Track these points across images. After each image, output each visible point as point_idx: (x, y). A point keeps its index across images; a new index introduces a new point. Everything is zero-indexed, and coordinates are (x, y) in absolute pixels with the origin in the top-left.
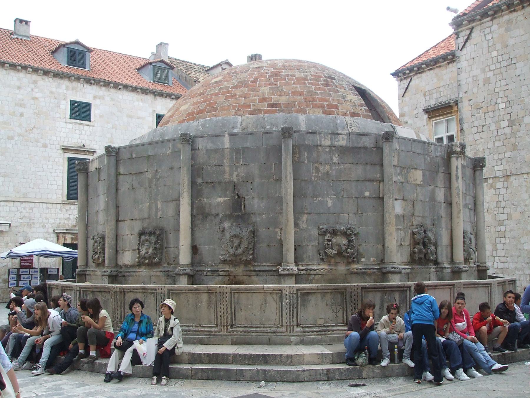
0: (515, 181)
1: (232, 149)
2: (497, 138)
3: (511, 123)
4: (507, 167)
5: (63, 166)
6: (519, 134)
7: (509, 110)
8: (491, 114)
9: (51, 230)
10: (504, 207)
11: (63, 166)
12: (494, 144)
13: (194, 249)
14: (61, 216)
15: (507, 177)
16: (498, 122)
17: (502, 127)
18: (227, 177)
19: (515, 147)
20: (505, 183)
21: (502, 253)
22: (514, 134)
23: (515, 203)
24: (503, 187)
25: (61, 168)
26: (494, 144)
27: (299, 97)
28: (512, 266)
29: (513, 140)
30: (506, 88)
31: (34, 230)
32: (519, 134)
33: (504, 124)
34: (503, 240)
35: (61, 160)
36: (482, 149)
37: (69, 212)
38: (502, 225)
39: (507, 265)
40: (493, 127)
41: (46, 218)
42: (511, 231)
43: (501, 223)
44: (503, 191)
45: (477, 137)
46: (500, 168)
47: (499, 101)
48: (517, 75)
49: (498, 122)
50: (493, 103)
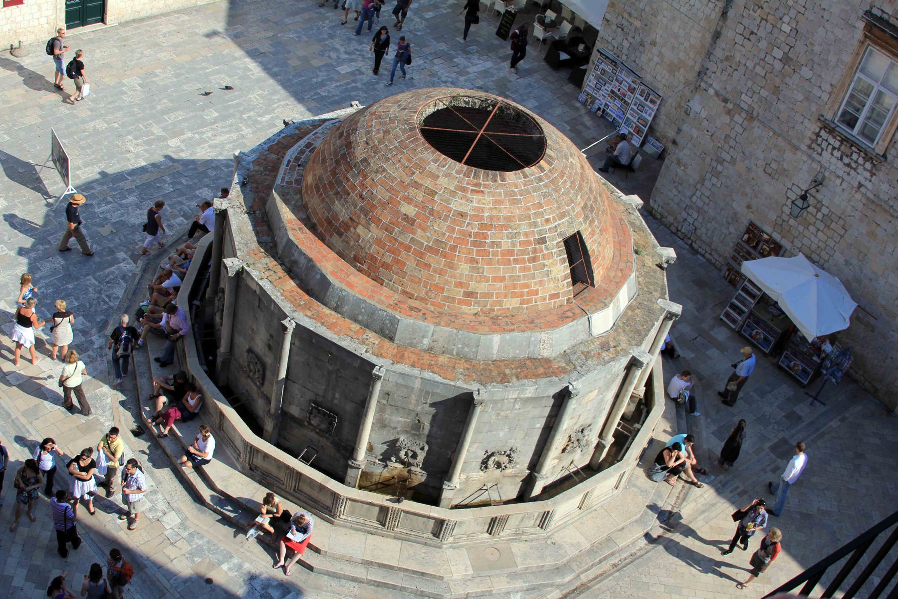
0: (757, 130)
1: (421, 390)
2: (762, 63)
3: (786, 60)
4: (756, 107)
6: (787, 80)
7: (791, 41)
8: (769, 27)
10: (731, 147)
12: (755, 67)
15: (751, 117)
16: (773, 45)
17: (773, 54)
18: (411, 407)
19: (776, 90)
20: (746, 122)
21: (707, 193)
23: (747, 153)
24: (741, 125)
26: (755, 67)
27: (498, 284)
28: (711, 213)
29: (777, 81)
30: (802, 10)
32: (787, 80)
33: (778, 53)
34: (714, 180)
36: (738, 60)
38: (721, 164)
39: (706, 208)
40: (763, 45)
43: (720, 161)
44: (740, 130)
45: (739, 39)
46: (749, 101)
47: (786, 19)
48: (823, 6)
49: (773, 45)
50: (778, 15)
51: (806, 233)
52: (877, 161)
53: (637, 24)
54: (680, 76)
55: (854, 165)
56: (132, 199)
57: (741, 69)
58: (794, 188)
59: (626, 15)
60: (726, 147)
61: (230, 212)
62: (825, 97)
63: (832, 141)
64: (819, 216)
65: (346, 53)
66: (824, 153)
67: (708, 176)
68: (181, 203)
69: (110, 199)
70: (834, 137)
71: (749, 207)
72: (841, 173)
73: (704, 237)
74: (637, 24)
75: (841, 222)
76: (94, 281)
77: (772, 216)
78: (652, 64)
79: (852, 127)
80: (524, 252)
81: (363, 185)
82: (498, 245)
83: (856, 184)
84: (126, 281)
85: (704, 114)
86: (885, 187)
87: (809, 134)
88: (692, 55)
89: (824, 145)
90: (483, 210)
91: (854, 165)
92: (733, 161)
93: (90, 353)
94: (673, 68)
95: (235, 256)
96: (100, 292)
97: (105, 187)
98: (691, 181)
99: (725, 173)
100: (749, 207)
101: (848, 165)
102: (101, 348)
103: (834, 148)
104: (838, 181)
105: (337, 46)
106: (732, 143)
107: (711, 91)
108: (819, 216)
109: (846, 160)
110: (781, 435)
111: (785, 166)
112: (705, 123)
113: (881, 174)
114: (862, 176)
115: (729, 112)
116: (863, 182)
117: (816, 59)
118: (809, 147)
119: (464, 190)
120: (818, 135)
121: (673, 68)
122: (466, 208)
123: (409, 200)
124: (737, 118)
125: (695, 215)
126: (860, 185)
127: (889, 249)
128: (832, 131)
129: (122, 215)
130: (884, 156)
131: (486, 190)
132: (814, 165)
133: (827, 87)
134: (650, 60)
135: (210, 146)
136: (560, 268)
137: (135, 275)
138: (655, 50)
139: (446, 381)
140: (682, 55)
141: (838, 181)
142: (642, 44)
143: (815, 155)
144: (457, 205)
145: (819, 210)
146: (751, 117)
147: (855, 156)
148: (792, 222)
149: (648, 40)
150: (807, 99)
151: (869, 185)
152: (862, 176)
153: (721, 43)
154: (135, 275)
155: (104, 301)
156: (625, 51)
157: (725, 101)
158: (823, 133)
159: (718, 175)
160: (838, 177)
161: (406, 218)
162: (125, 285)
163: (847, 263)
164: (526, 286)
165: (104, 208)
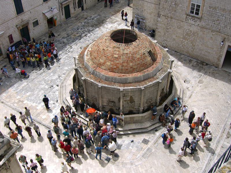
0: (174, 20)
3: (175, 4)
5: (13, 4)
6: (177, 8)
9: (15, 27)
11: (13, 4)
13: (123, 106)
14: (16, 21)
19: (175, 11)
22: (176, 8)
25: (12, 5)
29: (175, 9)
31: (10, 30)
32: (177, 8)
33: (173, 3)
34: (167, 33)
35: (12, 2)
37: (19, 19)
39: (167, 39)
41: (13, 24)
42: (170, 32)
43: (168, 29)
44: (170, 21)
45: (164, 3)
51: (190, 38)
52: (200, 19)
53: (140, 7)
54: (152, 15)
55: (196, 21)
56: (52, 74)
57: (167, 9)
58: (185, 30)
59: (137, 6)
60: (168, 26)
61: (78, 68)
62: (186, 9)
63: (190, 18)
64: (192, 33)
65: (82, 32)
66: (189, 20)
67: (166, 33)
68: (62, 72)
69: (47, 76)
70: (190, 17)
71: (176, 36)
72: (194, 23)
73: (169, 46)
74: (140, 7)
75: (197, 33)
76: (51, 93)
77: (182, 37)
78: (146, 14)
79: (193, 13)
80: (141, 57)
81: (104, 54)
82: (136, 57)
83: (197, 25)
84: (58, 91)
85: (161, 21)
86: (204, 23)
87: (185, 18)
88: (154, 10)
89: (188, 19)
90: (131, 51)
91: (196, 21)
92: (170, 28)
93: (57, 107)
94: (150, 14)
95: (83, 77)
96: (53, 95)
97: (45, 74)
98: (163, 35)
99: (169, 31)
100: (176, 36)
101: (195, 21)
102: (59, 106)
103: (191, 19)
104: (194, 25)
105: (80, 31)
106: (169, 24)
107: (162, 15)
108: (192, 33)
109: (194, 20)
110: (199, 79)
111: (182, 26)
112: (162, 22)
113: (202, 21)
114: (198, 23)
115: (166, 19)
116: (199, 24)
117: (182, 2)
118: (185, 20)
119: (126, 48)
120: (187, 17)
121: (150, 14)
122: (128, 52)
123: (115, 54)
124: (169, 19)
125: (166, 42)
126: (198, 25)
127: (208, 35)
128: (189, 15)
129: (51, 78)
130: (202, 17)
131: (130, 47)
132: (188, 24)
133: (186, 7)
134: (145, 14)
135: (63, 59)
136: (149, 59)
137: (59, 89)
138: (146, 11)
139: (135, 87)
140: (152, 11)
141: (194, 25)
142: (142, 11)
143: (187, 22)
144: (125, 52)
145: (191, 32)
146: (171, 18)
147: (196, 19)
148: (186, 36)
149: (143, 10)
150: (182, 11)
151: (200, 24)
152: (198, 23)
153: (161, 5)
154: (59, 89)
155: (56, 96)
156: (139, 13)
157: (165, 16)
158: (187, 17)
159: (168, 32)
160: (193, 24)
161: (116, 58)
162: (58, 92)
163: (200, 41)
164: (144, 64)
165: (47, 78)
